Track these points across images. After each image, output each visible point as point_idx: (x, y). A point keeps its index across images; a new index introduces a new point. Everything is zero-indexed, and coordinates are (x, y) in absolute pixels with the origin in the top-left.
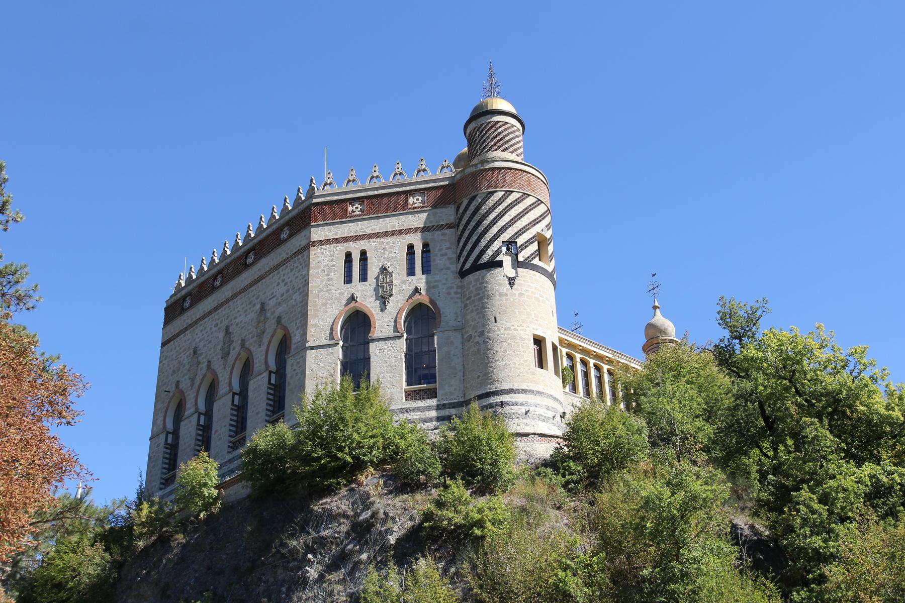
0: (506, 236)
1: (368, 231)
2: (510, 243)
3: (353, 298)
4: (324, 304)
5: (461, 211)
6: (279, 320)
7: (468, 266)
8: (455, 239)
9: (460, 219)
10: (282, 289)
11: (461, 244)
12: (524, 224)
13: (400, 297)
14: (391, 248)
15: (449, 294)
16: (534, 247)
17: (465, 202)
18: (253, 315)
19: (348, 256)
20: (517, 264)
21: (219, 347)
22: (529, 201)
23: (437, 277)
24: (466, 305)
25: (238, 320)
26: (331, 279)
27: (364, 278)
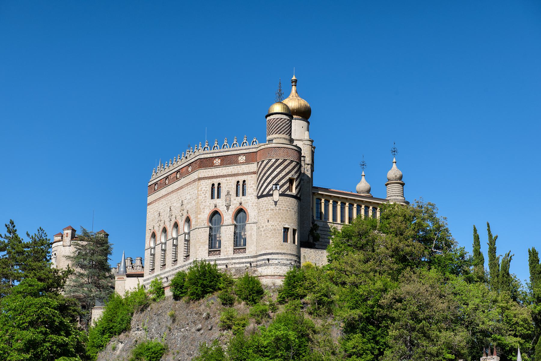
1: (221, 174)
2: (276, 184)
4: (204, 208)
7: (259, 195)
8: (256, 179)
12: (283, 175)
13: (233, 207)
14: (231, 182)
15: (252, 206)
16: (288, 184)
19: (213, 185)
23: (248, 198)
26: (206, 197)
27: (218, 197)
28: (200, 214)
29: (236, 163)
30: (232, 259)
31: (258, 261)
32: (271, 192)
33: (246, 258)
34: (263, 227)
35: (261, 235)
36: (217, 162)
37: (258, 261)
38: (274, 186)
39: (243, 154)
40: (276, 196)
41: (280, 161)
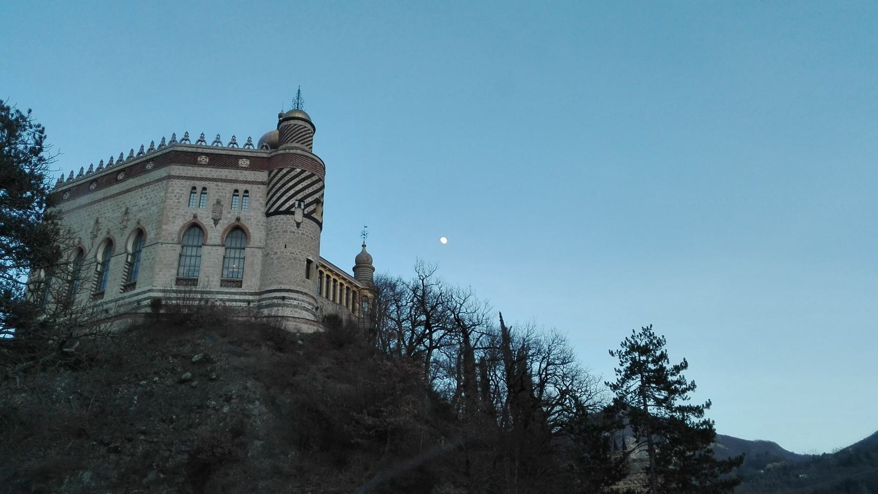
0: (299, 196)
1: (209, 176)
2: (301, 201)
3: (195, 217)
4: (174, 217)
5: (272, 175)
6: (138, 223)
7: (272, 210)
8: (265, 192)
9: (271, 181)
10: (144, 201)
11: (269, 196)
13: (226, 222)
17: (275, 171)
18: (118, 214)
19: (194, 188)
20: (305, 216)
21: (90, 231)
22: (314, 178)
24: (267, 234)
25: (107, 215)
26: (179, 202)
28: (166, 224)
29: (236, 167)
30: (218, 293)
31: (264, 299)
32: (293, 209)
33: (241, 294)
34: (276, 253)
35: (272, 263)
36: (204, 160)
37: (264, 299)
38: (297, 203)
39: (247, 157)
40: (299, 216)
41: (307, 173)
